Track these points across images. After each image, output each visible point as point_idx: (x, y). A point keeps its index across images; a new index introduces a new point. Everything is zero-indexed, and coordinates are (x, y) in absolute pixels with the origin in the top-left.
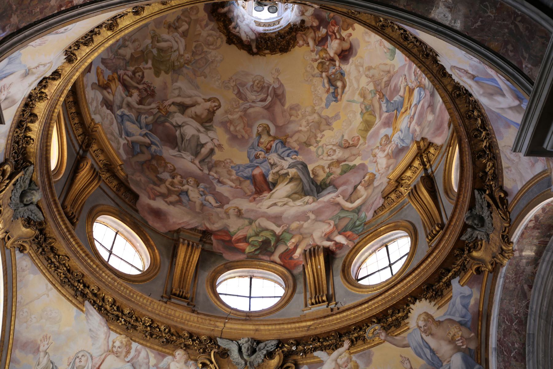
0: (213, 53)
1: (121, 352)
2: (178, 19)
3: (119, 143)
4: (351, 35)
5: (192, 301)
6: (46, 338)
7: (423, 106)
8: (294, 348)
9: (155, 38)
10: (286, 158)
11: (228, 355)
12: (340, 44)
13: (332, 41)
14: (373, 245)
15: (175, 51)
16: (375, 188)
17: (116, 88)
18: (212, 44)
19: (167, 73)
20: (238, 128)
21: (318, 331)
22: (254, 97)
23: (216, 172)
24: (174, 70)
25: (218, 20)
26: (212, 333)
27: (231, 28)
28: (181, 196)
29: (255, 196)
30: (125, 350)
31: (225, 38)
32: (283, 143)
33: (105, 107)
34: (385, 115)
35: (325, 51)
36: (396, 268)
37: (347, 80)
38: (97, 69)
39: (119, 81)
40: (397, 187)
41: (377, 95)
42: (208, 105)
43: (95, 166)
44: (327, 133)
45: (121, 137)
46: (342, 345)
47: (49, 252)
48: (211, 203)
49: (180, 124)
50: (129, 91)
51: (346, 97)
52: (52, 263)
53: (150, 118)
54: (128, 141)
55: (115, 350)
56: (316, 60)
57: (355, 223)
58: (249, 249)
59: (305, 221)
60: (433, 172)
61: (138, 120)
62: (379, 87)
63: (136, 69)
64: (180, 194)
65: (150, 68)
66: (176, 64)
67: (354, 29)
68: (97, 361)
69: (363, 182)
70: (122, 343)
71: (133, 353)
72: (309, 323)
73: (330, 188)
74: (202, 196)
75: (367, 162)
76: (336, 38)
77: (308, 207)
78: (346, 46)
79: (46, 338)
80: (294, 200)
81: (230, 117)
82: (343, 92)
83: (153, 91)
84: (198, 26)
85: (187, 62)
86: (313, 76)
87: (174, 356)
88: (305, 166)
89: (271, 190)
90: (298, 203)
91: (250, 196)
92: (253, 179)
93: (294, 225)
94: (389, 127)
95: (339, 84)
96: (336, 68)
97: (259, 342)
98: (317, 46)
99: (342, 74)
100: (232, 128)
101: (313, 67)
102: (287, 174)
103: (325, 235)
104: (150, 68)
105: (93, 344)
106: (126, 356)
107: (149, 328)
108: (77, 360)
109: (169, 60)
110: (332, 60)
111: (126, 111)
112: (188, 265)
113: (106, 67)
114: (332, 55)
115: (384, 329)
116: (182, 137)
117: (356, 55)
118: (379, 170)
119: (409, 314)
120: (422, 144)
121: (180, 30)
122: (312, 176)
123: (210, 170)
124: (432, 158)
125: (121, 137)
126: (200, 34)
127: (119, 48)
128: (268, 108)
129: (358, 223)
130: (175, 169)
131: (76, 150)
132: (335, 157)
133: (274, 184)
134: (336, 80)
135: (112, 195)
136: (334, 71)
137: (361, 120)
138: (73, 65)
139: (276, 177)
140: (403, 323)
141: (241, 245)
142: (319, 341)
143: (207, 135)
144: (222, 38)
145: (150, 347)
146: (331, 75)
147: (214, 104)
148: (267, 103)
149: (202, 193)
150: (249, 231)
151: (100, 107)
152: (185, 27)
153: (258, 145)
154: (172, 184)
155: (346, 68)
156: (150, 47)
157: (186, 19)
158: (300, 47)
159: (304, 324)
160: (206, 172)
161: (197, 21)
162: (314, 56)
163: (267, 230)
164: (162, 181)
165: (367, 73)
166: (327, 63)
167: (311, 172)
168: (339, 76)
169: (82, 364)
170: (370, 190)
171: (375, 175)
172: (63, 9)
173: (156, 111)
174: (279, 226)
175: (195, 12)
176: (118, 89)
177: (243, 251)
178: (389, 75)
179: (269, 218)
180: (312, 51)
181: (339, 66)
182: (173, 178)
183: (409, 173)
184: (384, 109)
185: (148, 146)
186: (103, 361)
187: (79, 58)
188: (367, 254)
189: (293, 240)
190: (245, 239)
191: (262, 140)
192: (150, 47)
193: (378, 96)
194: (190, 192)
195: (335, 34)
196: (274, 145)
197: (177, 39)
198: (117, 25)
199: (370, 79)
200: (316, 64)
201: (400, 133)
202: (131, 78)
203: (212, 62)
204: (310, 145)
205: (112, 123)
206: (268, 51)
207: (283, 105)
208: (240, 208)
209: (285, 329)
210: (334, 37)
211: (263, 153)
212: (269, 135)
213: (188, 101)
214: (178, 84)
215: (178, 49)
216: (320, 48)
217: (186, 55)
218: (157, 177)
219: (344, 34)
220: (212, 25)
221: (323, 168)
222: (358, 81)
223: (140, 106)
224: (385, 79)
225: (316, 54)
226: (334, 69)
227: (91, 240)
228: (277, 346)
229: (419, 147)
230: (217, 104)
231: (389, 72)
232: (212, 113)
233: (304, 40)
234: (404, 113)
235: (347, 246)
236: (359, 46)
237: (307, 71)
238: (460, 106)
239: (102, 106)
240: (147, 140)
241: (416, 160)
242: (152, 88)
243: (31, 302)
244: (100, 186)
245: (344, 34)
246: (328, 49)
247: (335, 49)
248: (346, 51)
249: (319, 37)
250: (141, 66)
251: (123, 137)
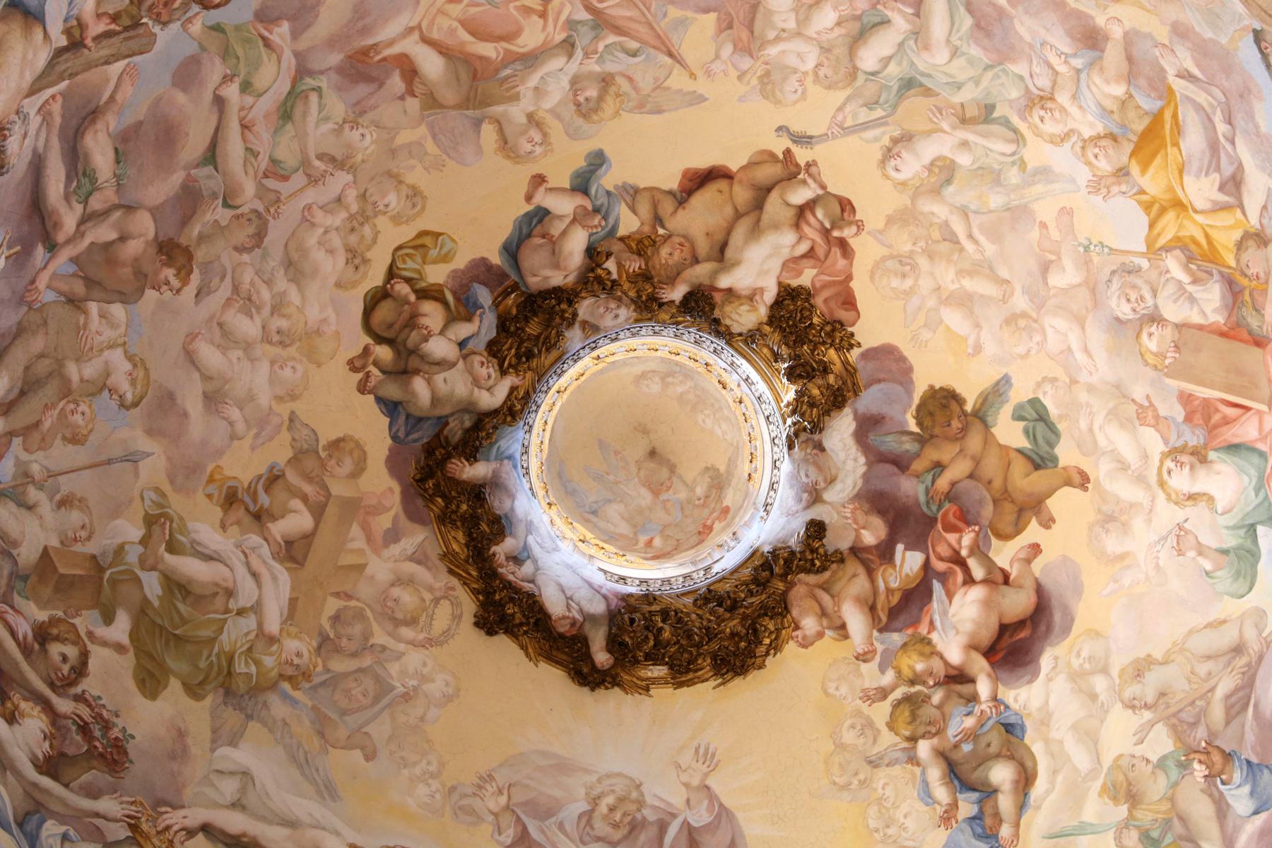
0: (414, 659)
2: (273, 479)
4: (1036, 549)
12: (987, 604)
13: (950, 595)
15: (241, 612)
18: (412, 622)
19: (194, 690)
24: (228, 692)
25: (444, 519)
27: (501, 558)
31: (469, 606)
35: (925, 645)
37: (1037, 748)
41: (1196, 765)
56: (883, 693)
63: (54, 621)
65: (120, 648)
66: (240, 667)
67: (1048, 523)
76: (969, 581)
78: (1018, 603)
82: (1021, 807)
83: (119, 747)
84: (355, 530)
85: (290, 671)
86: (873, 763)
95: (1001, 774)
96: (977, 710)
98: (881, 631)
99: (1011, 729)
101: (870, 724)
104: (120, 648)
109: (212, 641)
110: (958, 678)
114: (955, 655)
117: (1067, 630)
121: (278, 529)
126: (361, 568)
134: (984, 760)
136: (969, 722)
144: (455, 604)
146: (956, 746)
152: (297, 521)
156: (133, 556)
157: (308, 489)
158: (805, 644)
161: (352, 507)
162: (871, 675)
165: (1132, 690)
166: (937, 697)
168: (995, 739)
175: (348, 465)
178: (1241, 661)
180: (863, 657)
181: (995, 698)
192: (133, 556)
193: (1199, 770)
195: (962, 563)
197: (256, 564)
199: (1147, 715)
200: (885, 707)
202: (26, 650)
203: (406, 697)
206: (659, 671)
210: (960, 577)
214: (241, 756)
215: (257, 608)
216: (896, 638)
217: (292, 645)
219: (1004, 554)
220: (418, 537)
222: (1091, 738)
223: (46, 782)
225: (882, 669)
226: (969, 714)
231: (1238, 649)
233: (823, 613)
236: (1078, 590)
237: (841, 747)
242: (115, 733)
245: (1004, 554)
246: (934, 637)
247: (968, 627)
248: (1021, 624)
249: (889, 591)
250: (77, 621)
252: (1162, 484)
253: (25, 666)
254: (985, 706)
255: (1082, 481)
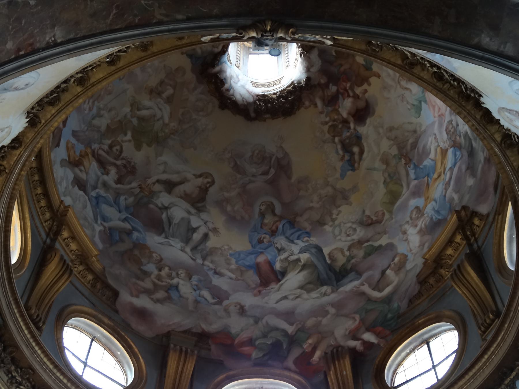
2: (162, 83)
3: (93, 230)
4: (366, 91)
7: (460, 169)
9: (135, 105)
10: (296, 241)
13: (344, 99)
14: (410, 343)
15: (158, 120)
16: (408, 271)
17: (90, 164)
19: (149, 145)
20: (236, 208)
22: (254, 170)
23: (212, 262)
27: (224, 91)
28: (170, 291)
29: (261, 289)
31: (216, 102)
32: (292, 224)
33: (76, 188)
34: (414, 183)
35: (337, 112)
36: (443, 370)
38: (68, 143)
39: (93, 156)
40: (435, 268)
41: (403, 160)
42: (200, 181)
43: (66, 257)
44: (344, 208)
45: (96, 222)
47: (9, 364)
48: (206, 300)
49: (166, 205)
50: (105, 168)
51: (365, 164)
52: (13, 377)
53: (131, 200)
54: (104, 227)
56: (326, 123)
57: (386, 315)
58: (255, 354)
59: (324, 316)
60: (479, 248)
61: (116, 202)
62: (404, 151)
63: (112, 142)
64: (169, 289)
66: (160, 135)
67: (369, 84)
69: (392, 266)
73: (352, 275)
74: (195, 290)
75: (395, 241)
76: (349, 96)
77: (326, 299)
78: (361, 104)
80: (309, 291)
81: (227, 195)
82: (360, 159)
83: (134, 167)
86: (324, 142)
88: (319, 250)
89: (279, 281)
90: (314, 294)
91: (254, 289)
92: (257, 268)
93: (310, 323)
94: (420, 197)
95: (356, 149)
96: (350, 131)
98: (326, 106)
100: (229, 208)
102: (298, 260)
103: (350, 332)
104: (129, 141)
110: (345, 122)
111: (102, 192)
112: (181, 376)
113: (78, 140)
114: (345, 115)
116: (170, 220)
117: (373, 114)
118: (411, 250)
120: (463, 213)
121: (164, 95)
122: (329, 261)
123: (204, 259)
124: (477, 230)
125: (96, 222)
127: (93, 119)
128: (272, 182)
129: (389, 316)
130: (161, 260)
131: (42, 239)
132: (355, 237)
133: (284, 273)
135: (86, 293)
136: (348, 134)
137: (385, 191)
138: (36, 130)
139: (286, 264)
141: (246, 349)
143: (199, 217)
146: (345, 140)
147: (206, 181)
148: (270, 176)
149: (195, 287)
150: (255, 332)
151: (71, 187)
152: (170, 91)
153: (261, 227)
154: (159, 277)
155: (362, 130)
156: (129, 116)
158: (306, 108)
160: (200, 261)
162: (323, 118)
163: (277, 329)
164: (147, 274)
166: (340, 126)
167: (327, 257)
170: (402, 275)
171: (406, 256)
172: (22, 53)
173: (138, 190)
174: (291, 324)
176: (93, 166)
177: (248, 357)
179: (279, 314)
180: (322, 113)
181: (355, 129)
182: (160, 270)
183: (450, 251)
184: (412, 175)
185: (129, 233)
187: (43, 121)
188: (403, 354)
189: (310, 341)
190: (250, 342)
191: (266, 221)
192: (129, 116)
193: (403, 161)
194: (180, 287)
195: (347, 91)
196: (281, 226)
198: (89, 79)
199: (392, 142)
200: (326, 128)
201: (433, 203)
202: (107, 153)
204: (325, 224)
205: (85, 207)
207: (289, 177)
208: (243, 303)
210: (346, 95)
211: (268, 236)
212: (274, 214)
213: (175, 178)
214: (163, 158)
215: (162, 118)
216: (330, 109)
217: (172, 124)
218: (141, 270)
219: (358, 91)
221: (342, 251)
223: (119, 186)
224: (411, 141)
225: (326, 117)
226: (348, 132)
227: (60, 349)
229: (459, 218)
230: (209, 180)
231: (415, 131)
232: (204, 190)
234: (436, 179)
235: (378, 345)
238: (512, 159)
239: (74, 187)
240: (127, 226)
241: (457, 233)
242: (132, 164)
244: (71, 282)
245: (358, 91)
246: (340, 110)
250: (119, 139)
251: (99, 222)
252: (399, 83)
253: (108, 158)
254: (352, 130)
255: (379, 76)
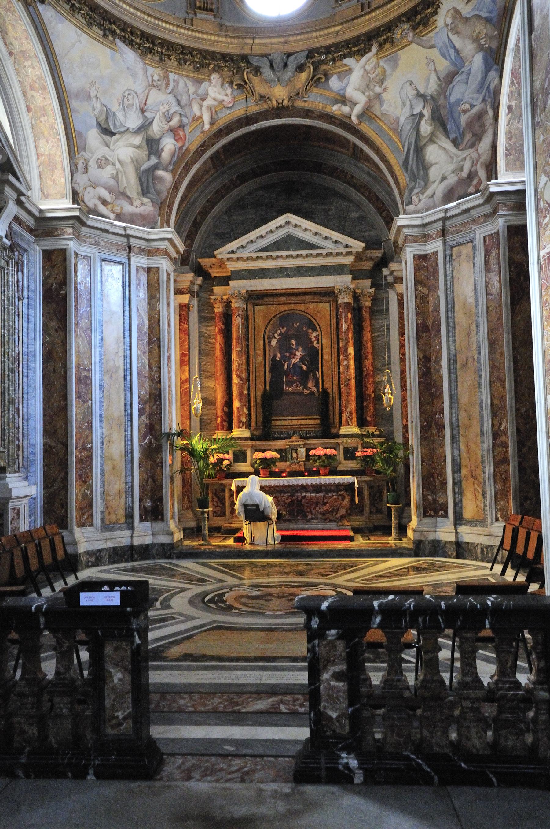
1: (161, 85)
5: (218, 12)
6: (92, 84)
8: (323, 57)
11: (261, 73)
21: (346, 37)
26: (242, 52)
30: (164, 82)
46: (370, 50)
55: (155, 83)
68: (142, 97)
70: (159, 76)
71: (172, 84)
72: (337, 28)
79: (92, 84)
87: (209, 80)
97: (289, 55)
105: (135, 82)
106: (166, 88)
107: (181, 56)
108: (125, 99)
115: (413, 28)
119: (439, 10)
140: (431, 20)
142: (348, 47)
145: (186, 76)
159: (332, 30)
169: (130, 102)
186: (148, 96)
209: (313, 38)
228: (307, 57)
243: (68, 52)
